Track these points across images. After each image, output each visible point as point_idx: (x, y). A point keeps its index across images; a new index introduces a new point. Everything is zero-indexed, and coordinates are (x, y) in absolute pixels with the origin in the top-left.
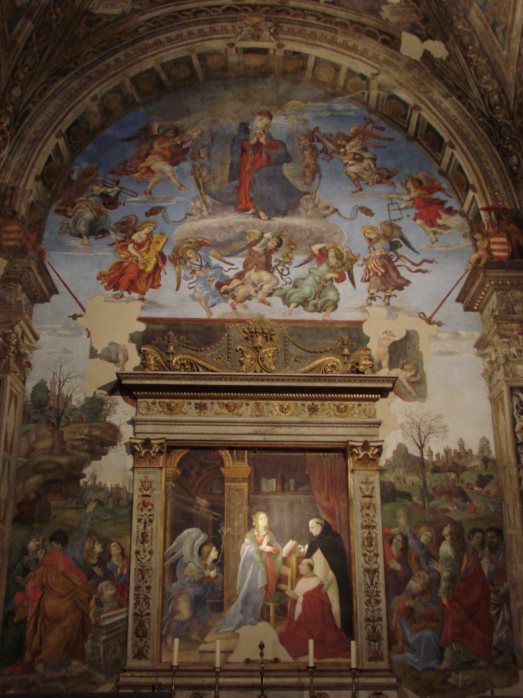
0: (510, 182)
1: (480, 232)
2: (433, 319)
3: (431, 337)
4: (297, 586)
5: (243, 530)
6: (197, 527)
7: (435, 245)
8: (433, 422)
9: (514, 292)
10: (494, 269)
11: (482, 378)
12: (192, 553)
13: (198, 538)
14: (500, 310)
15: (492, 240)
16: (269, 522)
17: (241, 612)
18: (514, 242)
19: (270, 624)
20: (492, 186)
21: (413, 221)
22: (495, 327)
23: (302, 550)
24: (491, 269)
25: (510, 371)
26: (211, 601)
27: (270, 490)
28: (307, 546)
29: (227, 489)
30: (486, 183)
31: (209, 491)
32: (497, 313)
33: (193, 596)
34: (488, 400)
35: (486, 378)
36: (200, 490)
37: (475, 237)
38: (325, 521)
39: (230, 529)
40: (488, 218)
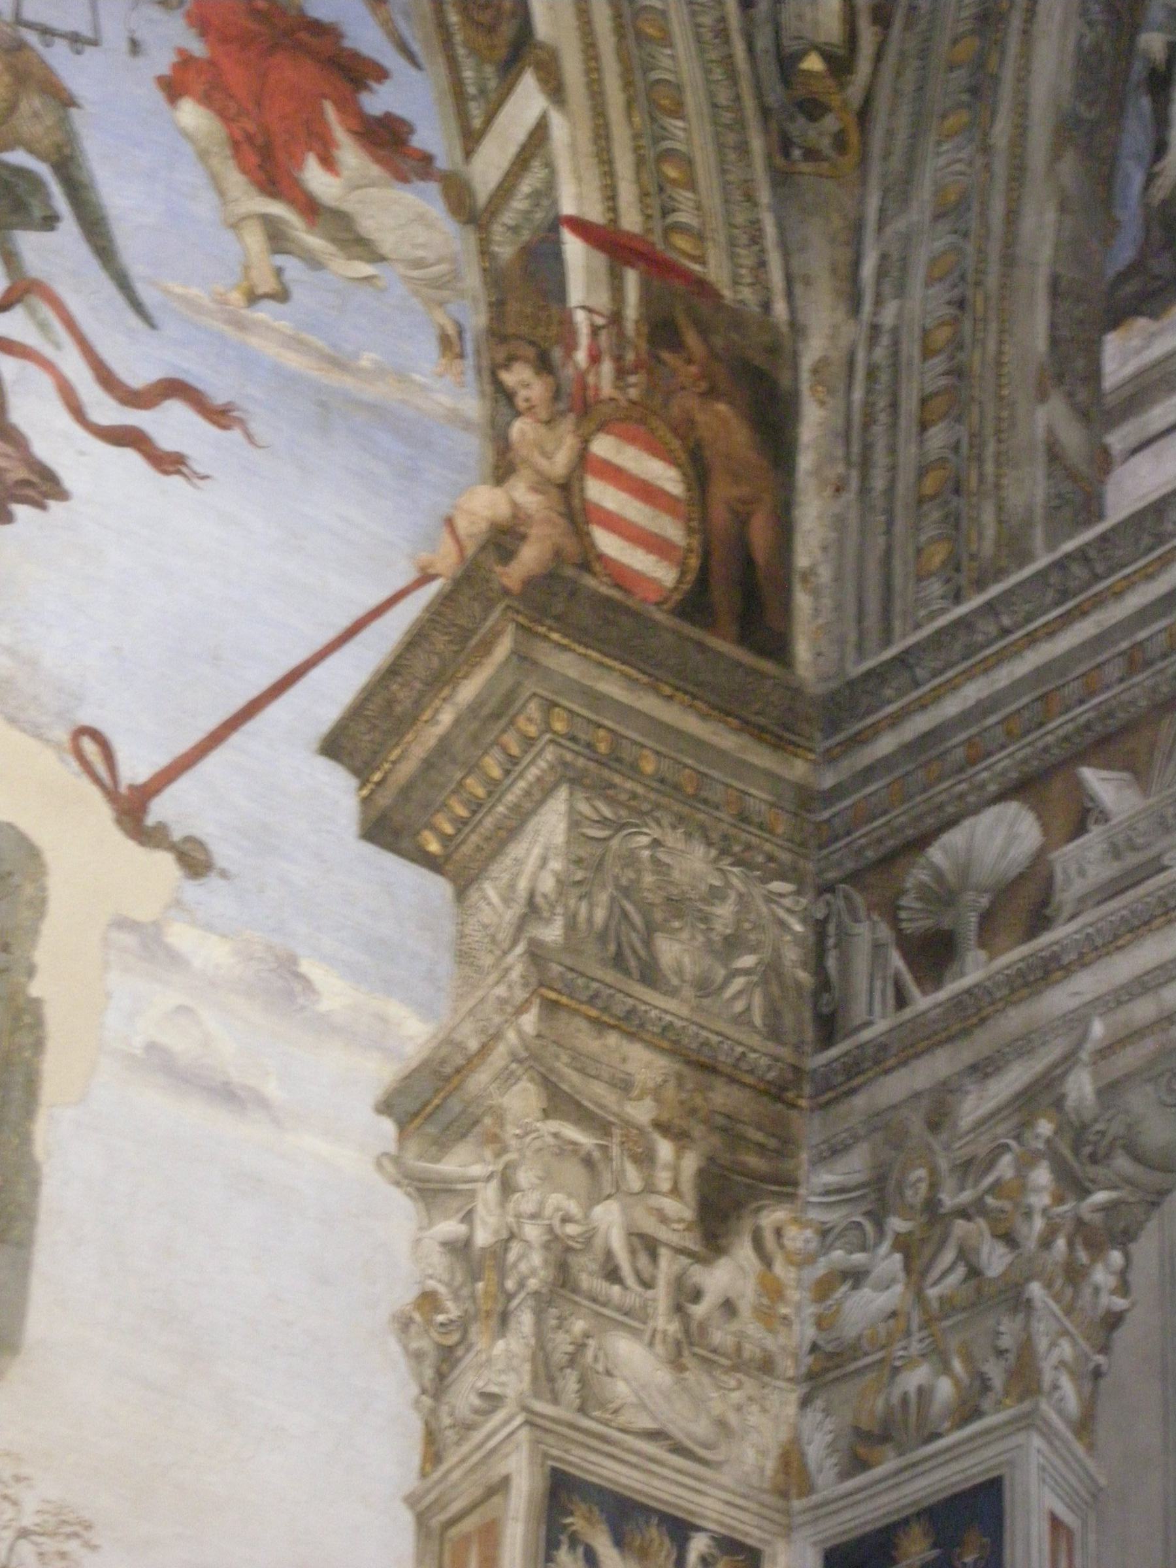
0: (757, 144)
1: (544, 365)
2: (160, 810)
3: (123, 924)
7: (264, 313)
8: (25, 1549)
9: (674, 838)
10: (582, 636)
11: (394, 1346)
14: (571, 925)
15: (603, 446)
18: (720, 515)
20: (654, 111)
21: (158, 97)
22: (529, 1021)
24: (561, 621)
25: (573, 1360)
30: (628, 84)
32: (552, 933)
34: (407, 1518)
35: (417, 1356)
37: (509, 378)
40: (602, 300)
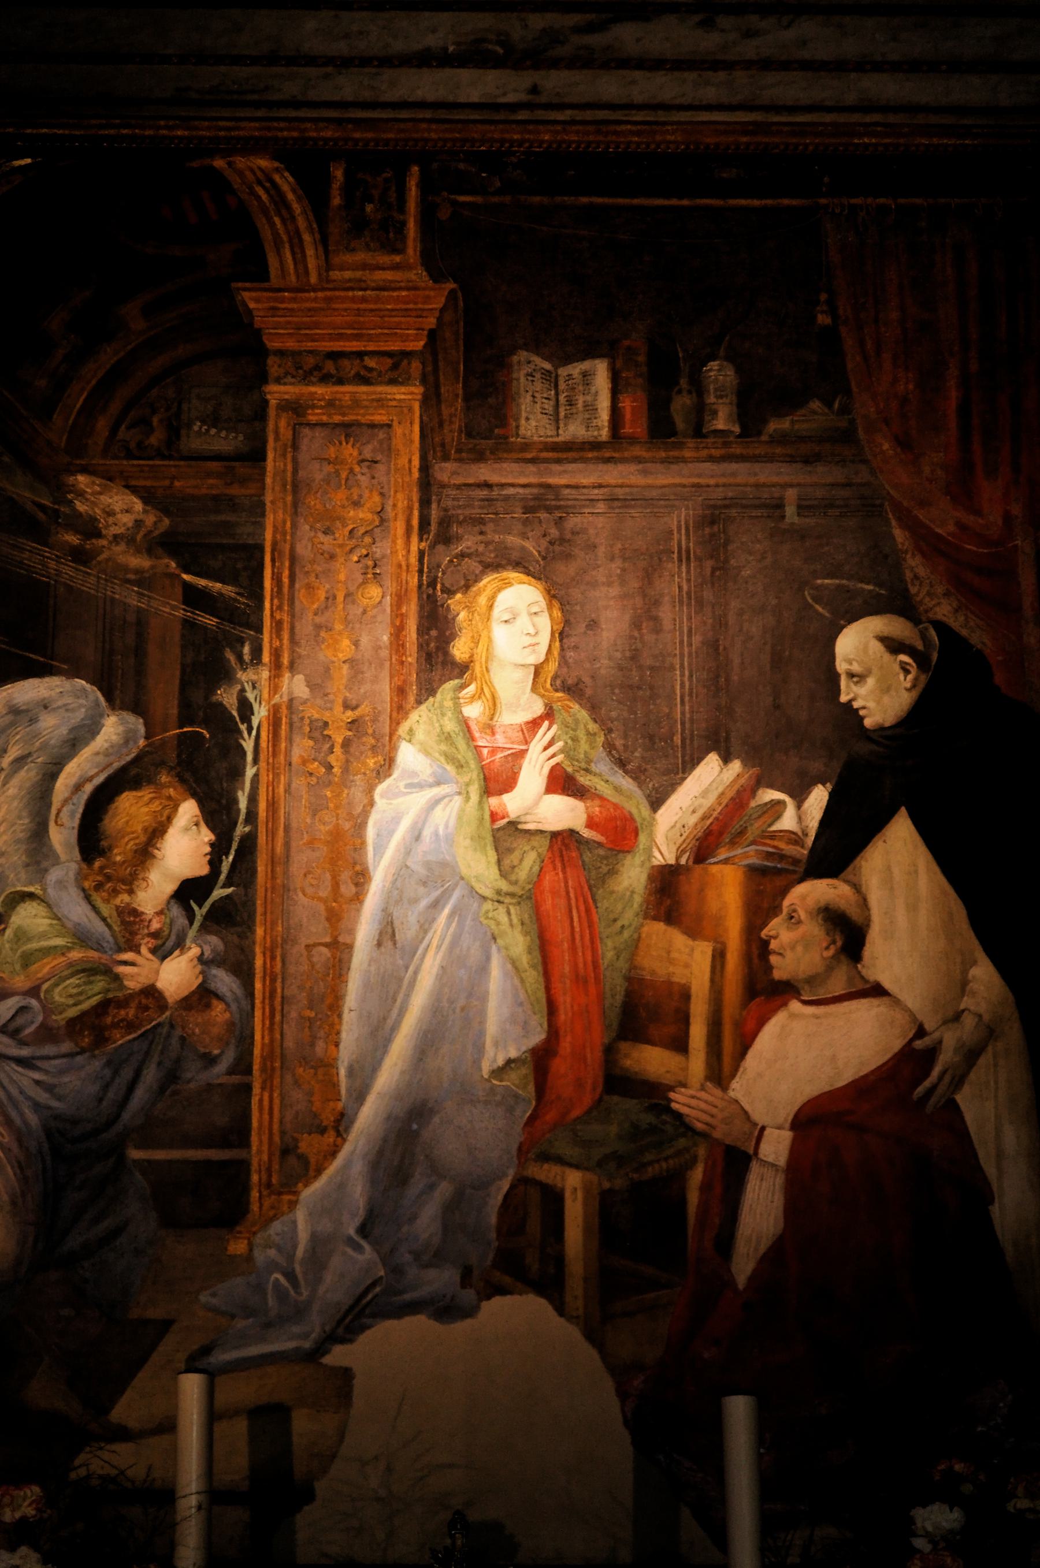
4: (752, 1061)
5: (385, 689)
6: (73, 673)
12: (39, 833)
13: (74, 743)
16: (561, 634)
17: (363, 1230)
19: (561, 1310)
23: (788, 822)
26: (160, 1155)
27: (574, 430)
28: (818, 798)
29: (278, 426)
31: (155, 440)
33: (33, 1119)
36: (102, 425)
38: (941, 627)
39: (296, 685)
